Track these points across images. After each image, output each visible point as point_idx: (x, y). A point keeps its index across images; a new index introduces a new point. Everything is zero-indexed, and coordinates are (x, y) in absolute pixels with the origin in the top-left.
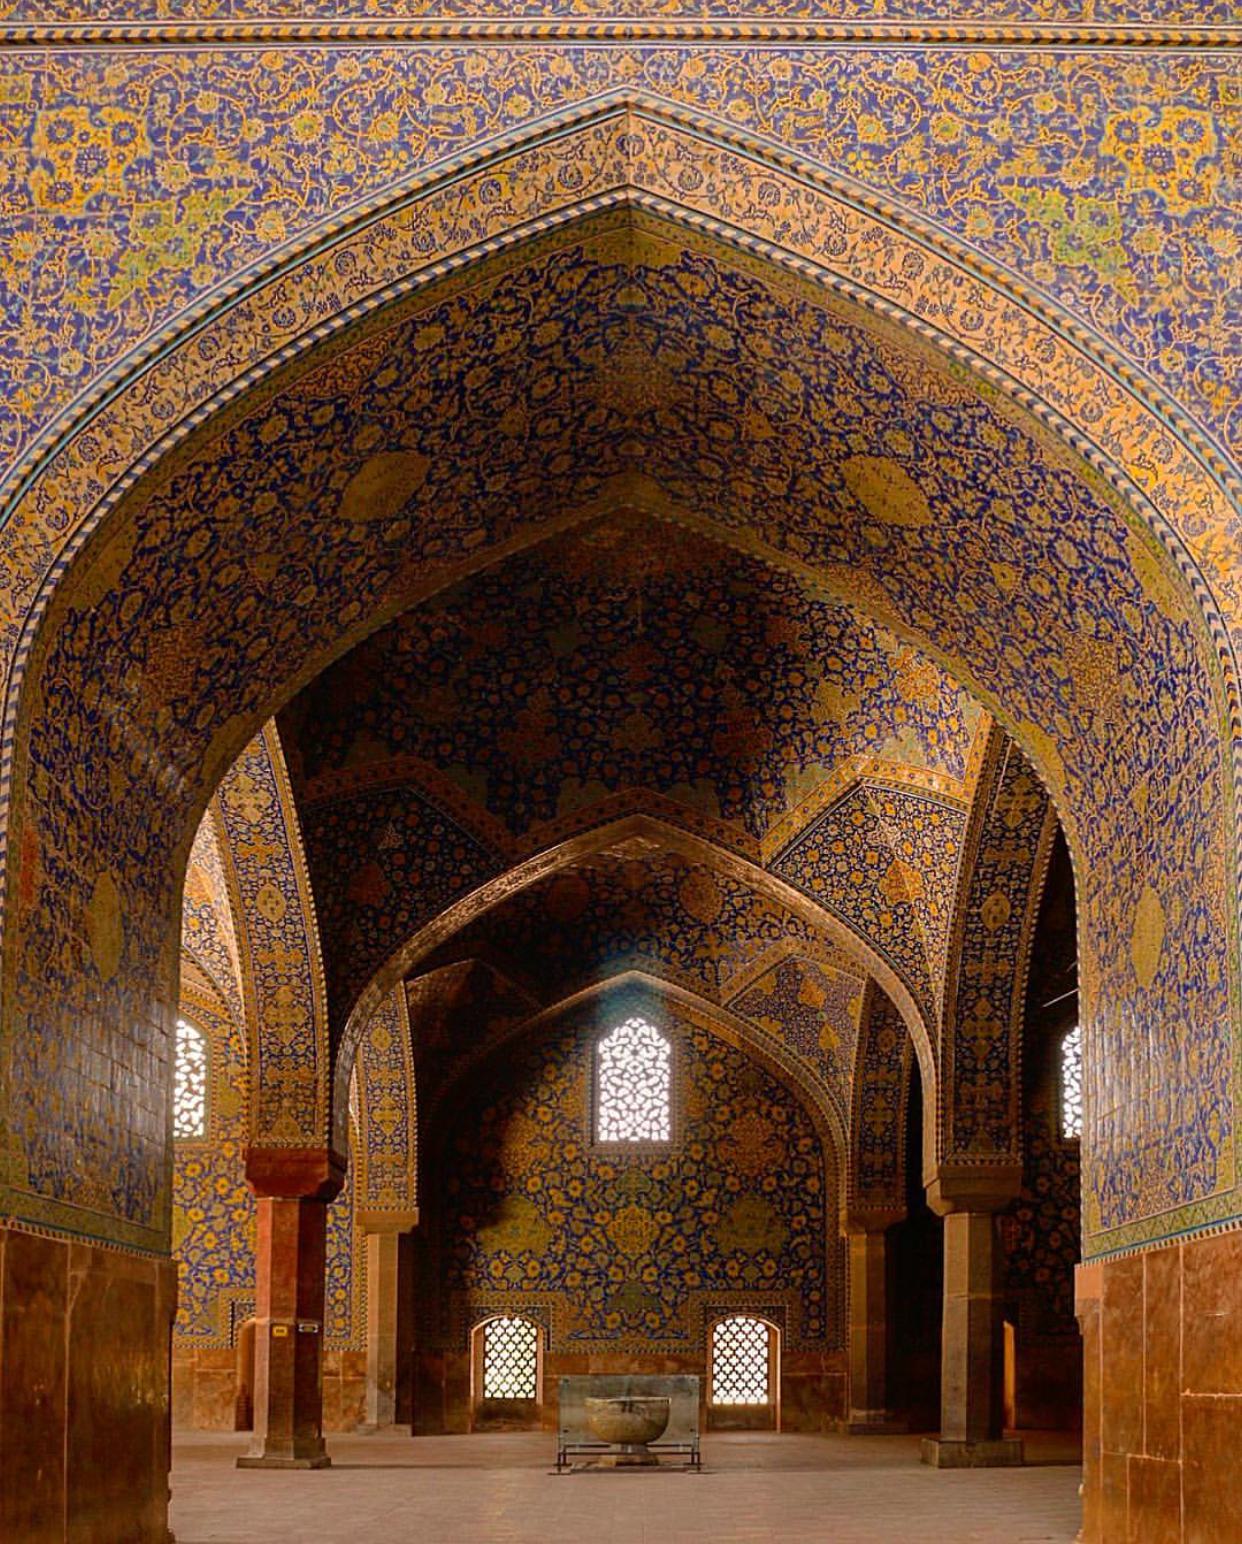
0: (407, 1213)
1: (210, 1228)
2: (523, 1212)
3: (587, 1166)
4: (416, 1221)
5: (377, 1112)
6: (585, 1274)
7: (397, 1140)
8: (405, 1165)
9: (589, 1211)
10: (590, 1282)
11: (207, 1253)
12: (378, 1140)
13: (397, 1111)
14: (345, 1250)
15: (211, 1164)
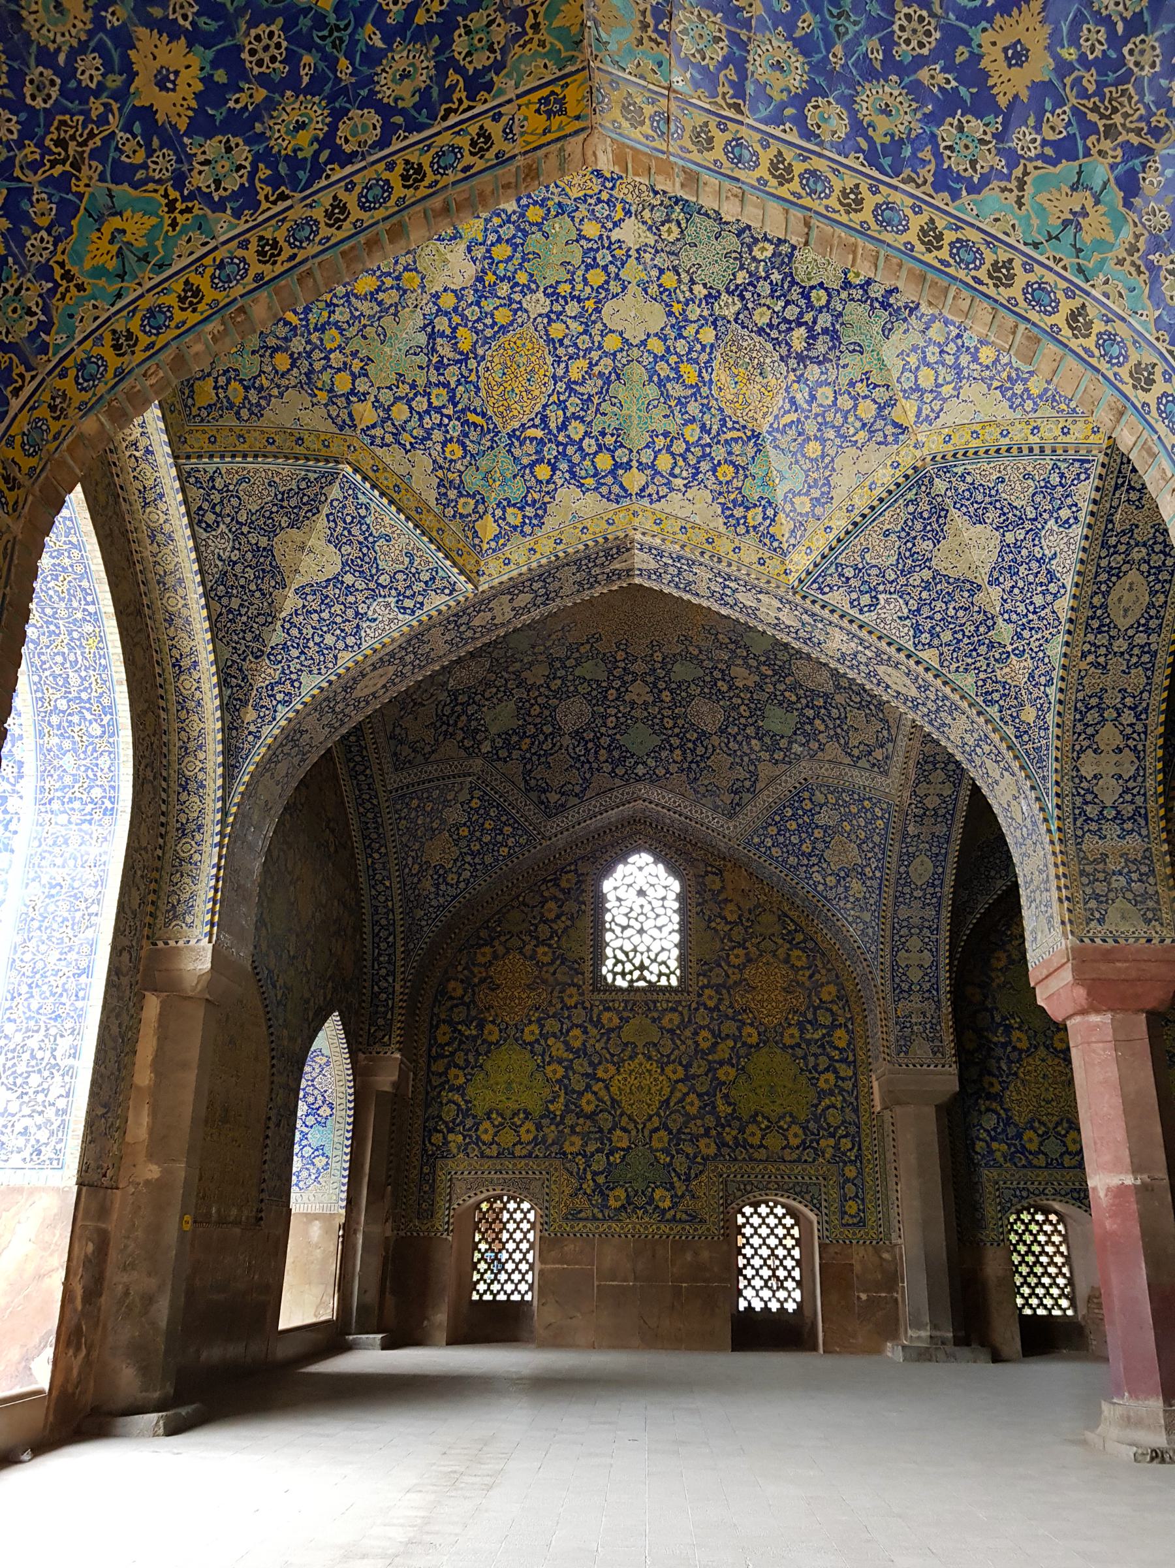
14: (850, 1116)
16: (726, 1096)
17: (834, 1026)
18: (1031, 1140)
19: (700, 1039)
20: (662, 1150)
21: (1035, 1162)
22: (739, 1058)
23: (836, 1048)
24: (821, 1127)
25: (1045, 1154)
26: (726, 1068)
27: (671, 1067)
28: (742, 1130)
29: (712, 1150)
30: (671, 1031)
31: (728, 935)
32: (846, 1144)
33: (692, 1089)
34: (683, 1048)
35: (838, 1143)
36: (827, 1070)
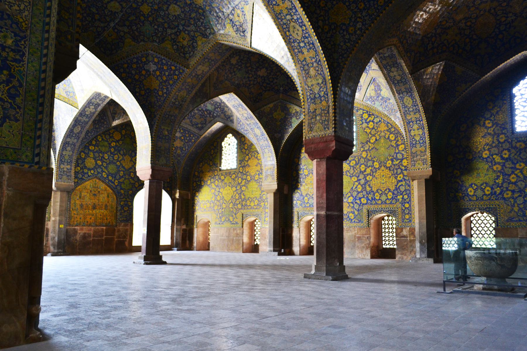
0: (427, 170)
1: (359, 183)
2: (483, 166)
3: (511, 143)
4: (431, 174)
5: (412, 131)
6: (513, 192)
7: (421, 141)
8: (425, 151)
9: (513, 163)
10: (516, 195)
11: (358, 193)
12: (414, 142)
13: (420, 130)
14: (408, 188)
15: (359, 160)
16: (369, 185)
17: (402, 160)
18: (471, 191)
19: (361, 168)
20: (351, 202)
21: (472, 199)
22: (373, 172)
23: (403, 166)
24: (398, 192)
25: (476, 196)
26: (369, 176)
27: (353, 177)
28: (374, 194)
29: (365, 202)
30: (353, 166)
31: (370, 133)
32: (406, 197)
33: (359, 183)
34: (356, 171)
35: (403, 197)
36: (400, 174)
